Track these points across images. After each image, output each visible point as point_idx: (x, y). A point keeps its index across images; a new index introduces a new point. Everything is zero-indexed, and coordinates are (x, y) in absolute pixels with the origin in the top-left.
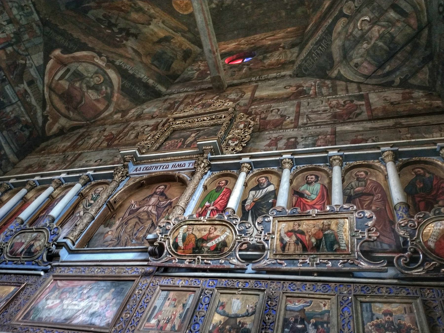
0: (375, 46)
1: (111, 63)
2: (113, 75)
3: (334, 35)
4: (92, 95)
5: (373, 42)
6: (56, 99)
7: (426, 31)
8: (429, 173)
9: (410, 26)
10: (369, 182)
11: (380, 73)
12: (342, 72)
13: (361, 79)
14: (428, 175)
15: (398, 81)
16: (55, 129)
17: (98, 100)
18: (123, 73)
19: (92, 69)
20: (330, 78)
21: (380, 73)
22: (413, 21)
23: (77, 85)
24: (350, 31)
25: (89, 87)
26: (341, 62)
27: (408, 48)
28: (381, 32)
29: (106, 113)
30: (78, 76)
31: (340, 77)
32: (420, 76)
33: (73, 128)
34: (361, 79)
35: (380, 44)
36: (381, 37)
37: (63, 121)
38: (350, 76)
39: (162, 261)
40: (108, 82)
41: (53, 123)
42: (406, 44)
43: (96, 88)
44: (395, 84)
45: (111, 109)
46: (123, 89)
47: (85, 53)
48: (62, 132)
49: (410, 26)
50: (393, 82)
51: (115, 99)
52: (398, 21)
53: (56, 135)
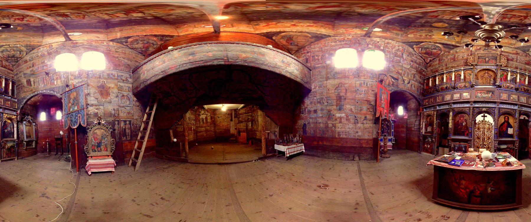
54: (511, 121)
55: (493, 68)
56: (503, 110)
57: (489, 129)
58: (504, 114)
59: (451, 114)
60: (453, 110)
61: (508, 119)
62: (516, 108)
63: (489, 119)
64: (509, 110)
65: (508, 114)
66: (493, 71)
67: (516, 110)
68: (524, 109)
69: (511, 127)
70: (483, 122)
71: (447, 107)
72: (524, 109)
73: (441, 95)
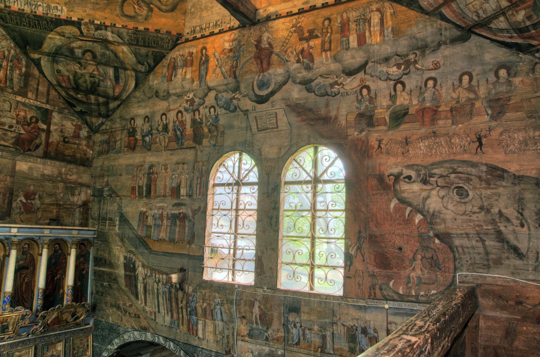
0: (83, 75)
3: (59, 29)
5: (84, 71)
8: (61, 250)
9: (114, 91)
10: (29, 255)
11: (72, 93)
12: (43, 63)
13: (55, 82)
14: (60, 251)
15: (78, 109)
20: (26, 54)
21: (72, 93)
22: (117, 91)
24: (74, 45)
26: (48, 54)
27: (101, 100)
28: (95, 73)
31: (37, 63)
32: (94, 120)
34: (55, 82)
35: (87, 77)
36: (92, 76)
38: (47, 71)
42: (103, 96)
44: (75, 109)
49: (114, 91)
50: (75, 107)
52: (110, 79)
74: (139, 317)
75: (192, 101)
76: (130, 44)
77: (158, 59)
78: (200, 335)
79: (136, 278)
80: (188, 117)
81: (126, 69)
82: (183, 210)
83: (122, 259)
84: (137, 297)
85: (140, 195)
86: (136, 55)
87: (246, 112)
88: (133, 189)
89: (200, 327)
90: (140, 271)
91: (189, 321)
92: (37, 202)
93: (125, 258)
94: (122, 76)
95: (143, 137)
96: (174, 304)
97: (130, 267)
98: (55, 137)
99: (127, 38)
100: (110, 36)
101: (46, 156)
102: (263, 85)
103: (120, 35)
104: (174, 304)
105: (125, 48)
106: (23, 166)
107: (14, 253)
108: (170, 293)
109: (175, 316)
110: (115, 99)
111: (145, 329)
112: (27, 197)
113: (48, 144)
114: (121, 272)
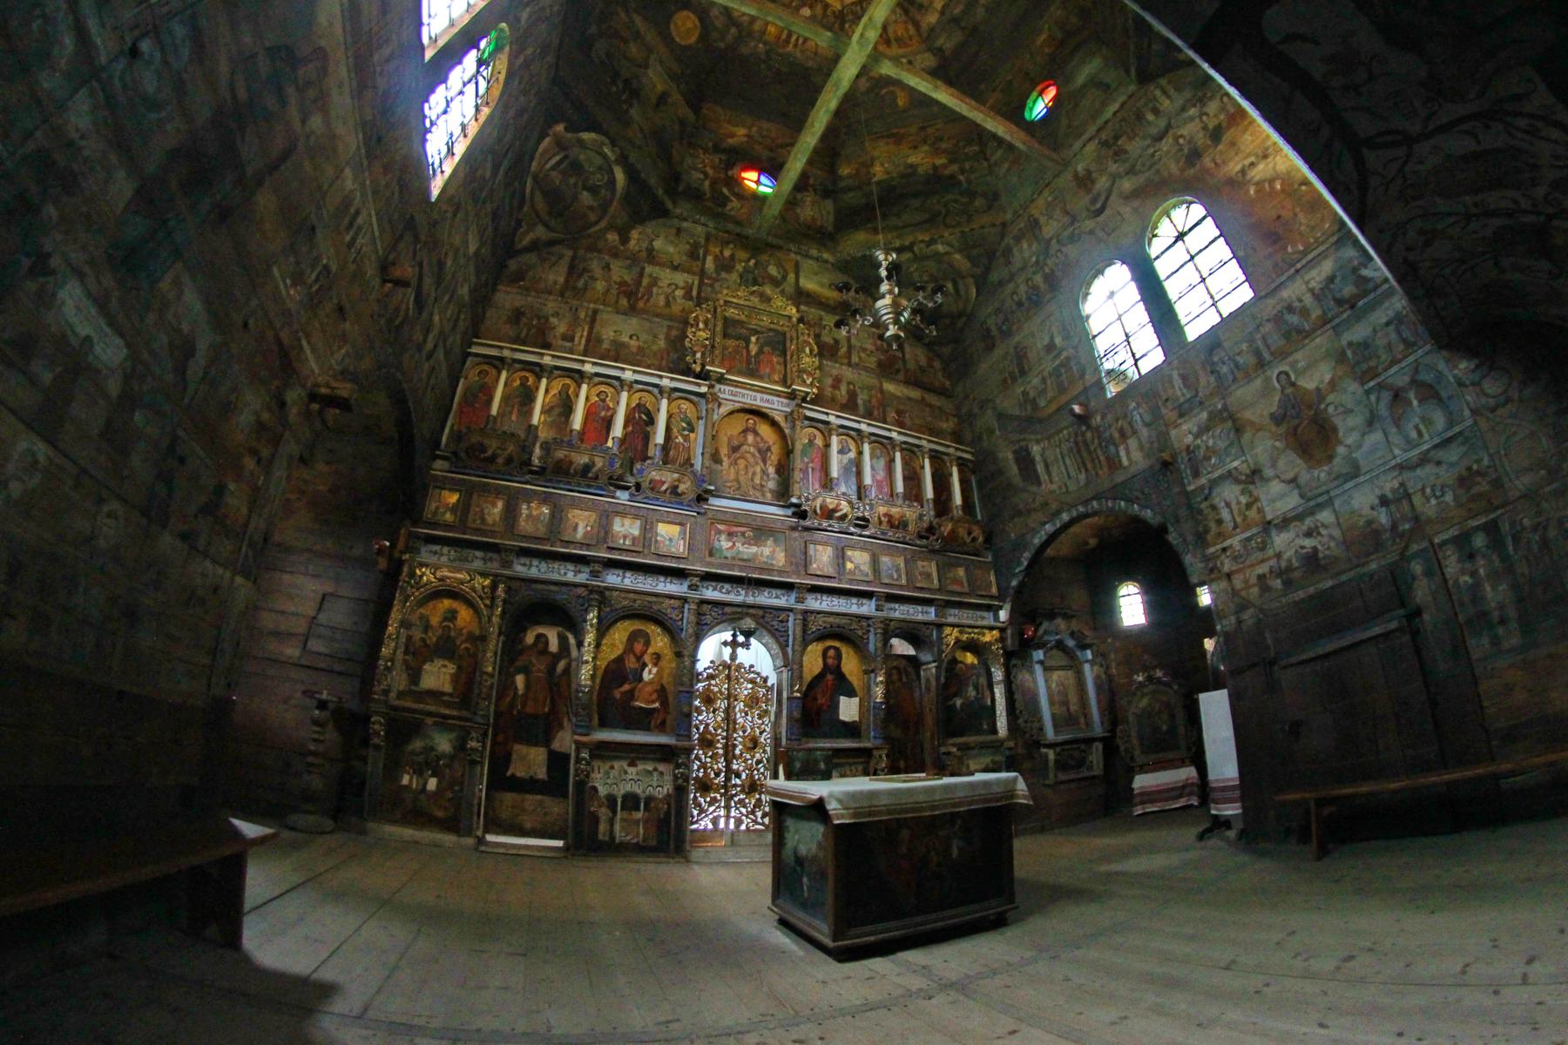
1: (623, 160)
2: (620, 175)
4: (586, 198)
6: (538, 198)
7: (964, 319)
16: (526, 241)
17: (591, 208)
18: (633, 175)
19: (598, 161)
23: (572, 181)
25: (585, 188)
29: (597, 228)
30: (576, 167)
33: (551, 243)
37: (540, 232)
39: (808, 523)
40: (612, 182)
41: (526, 233)
43: (594, 190)
45: (603, 224)
46: (627, 198)
47: (593, 135)
48: (534, 246)
51: (612, 209)
53: (528, 249)
54: (851, 665)
55: (777, 406)
56: (821, 619)
57: (753, 701)
58: (821, 638)
59: (592, 616)
60: (601, 596)
61: (839, 657)
62: (867, 608)
63: (758, 657)
64: (844, 621)
65: (841, 633)
66: (774, 424)
67: (868, 618)
68: (900, 612)
69: (851, 693)
70: (729, 670)
71: (569, 574)
72: (900, 612)
73: (546, 499)
74: (1047, 504)
75: (1037, 262)
76: (960, 251)
77: (991, 255)
78: (1125, 462)
79: (1032, 461)
80: (1038, 279)
81: (963, 278)
82: (1064, 354)
83: (1010, 456)
84: (1039, 484)
85: (1014, 379)
86: (969, 257)
87: (1091, 232)
88: (1005, 381)
89: (1122, 453)
90: (1036, 449)
91: (1108, 458)
92: (908, 422)
93: (1015, 452)
94: (961, 286)
95: (1000, 329)
96: (1085, 454)
97: (1025, 461)
98: (911, 365)
99: (956, 244)
100: (940, 248)
101: (907, 383)
102: (1094, 201)
103: (948, 244)
104: (1085, 454)
105: (958, 256)
106: (890, 387)
107: (898, 455)
108: (1076, 443)
109: (1089, 466)
110: (960, 315)
111: (1058, 512)
112: (899, 412)
113: (907, 371)
114: (1014, 470)
